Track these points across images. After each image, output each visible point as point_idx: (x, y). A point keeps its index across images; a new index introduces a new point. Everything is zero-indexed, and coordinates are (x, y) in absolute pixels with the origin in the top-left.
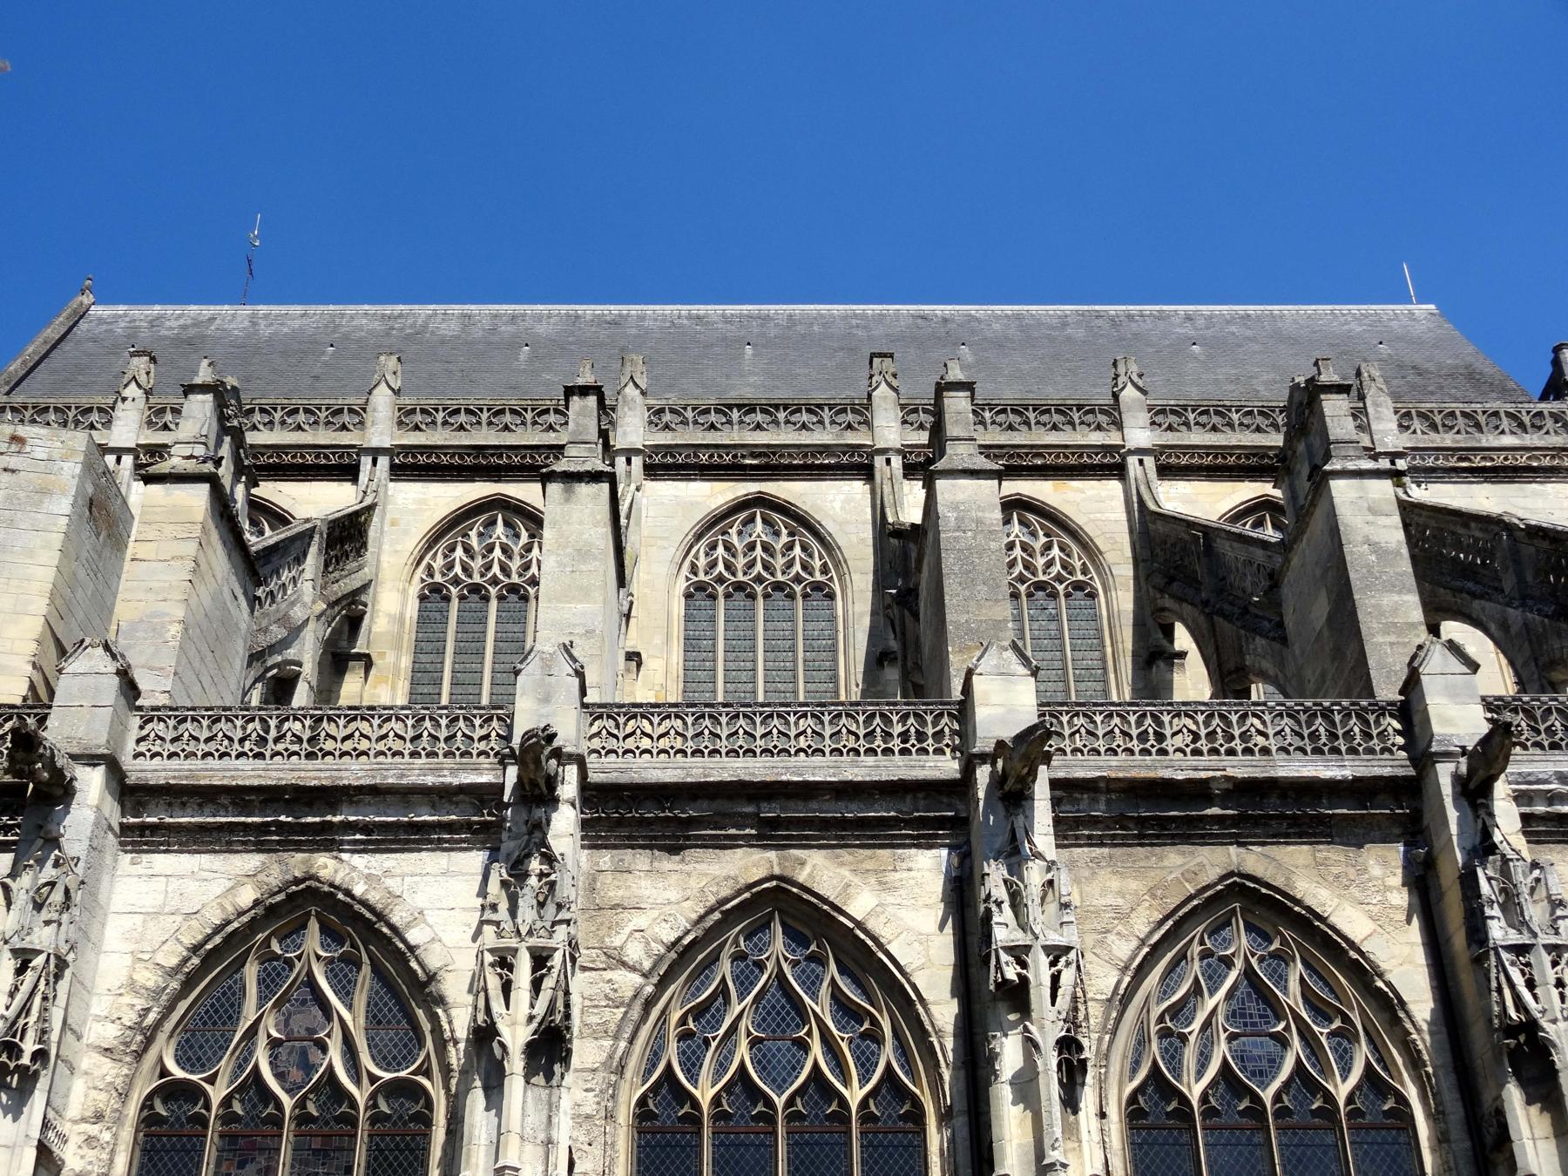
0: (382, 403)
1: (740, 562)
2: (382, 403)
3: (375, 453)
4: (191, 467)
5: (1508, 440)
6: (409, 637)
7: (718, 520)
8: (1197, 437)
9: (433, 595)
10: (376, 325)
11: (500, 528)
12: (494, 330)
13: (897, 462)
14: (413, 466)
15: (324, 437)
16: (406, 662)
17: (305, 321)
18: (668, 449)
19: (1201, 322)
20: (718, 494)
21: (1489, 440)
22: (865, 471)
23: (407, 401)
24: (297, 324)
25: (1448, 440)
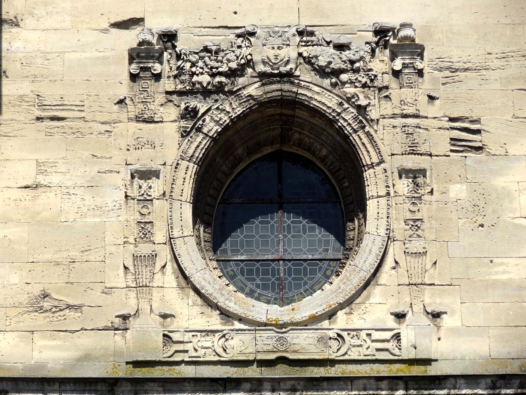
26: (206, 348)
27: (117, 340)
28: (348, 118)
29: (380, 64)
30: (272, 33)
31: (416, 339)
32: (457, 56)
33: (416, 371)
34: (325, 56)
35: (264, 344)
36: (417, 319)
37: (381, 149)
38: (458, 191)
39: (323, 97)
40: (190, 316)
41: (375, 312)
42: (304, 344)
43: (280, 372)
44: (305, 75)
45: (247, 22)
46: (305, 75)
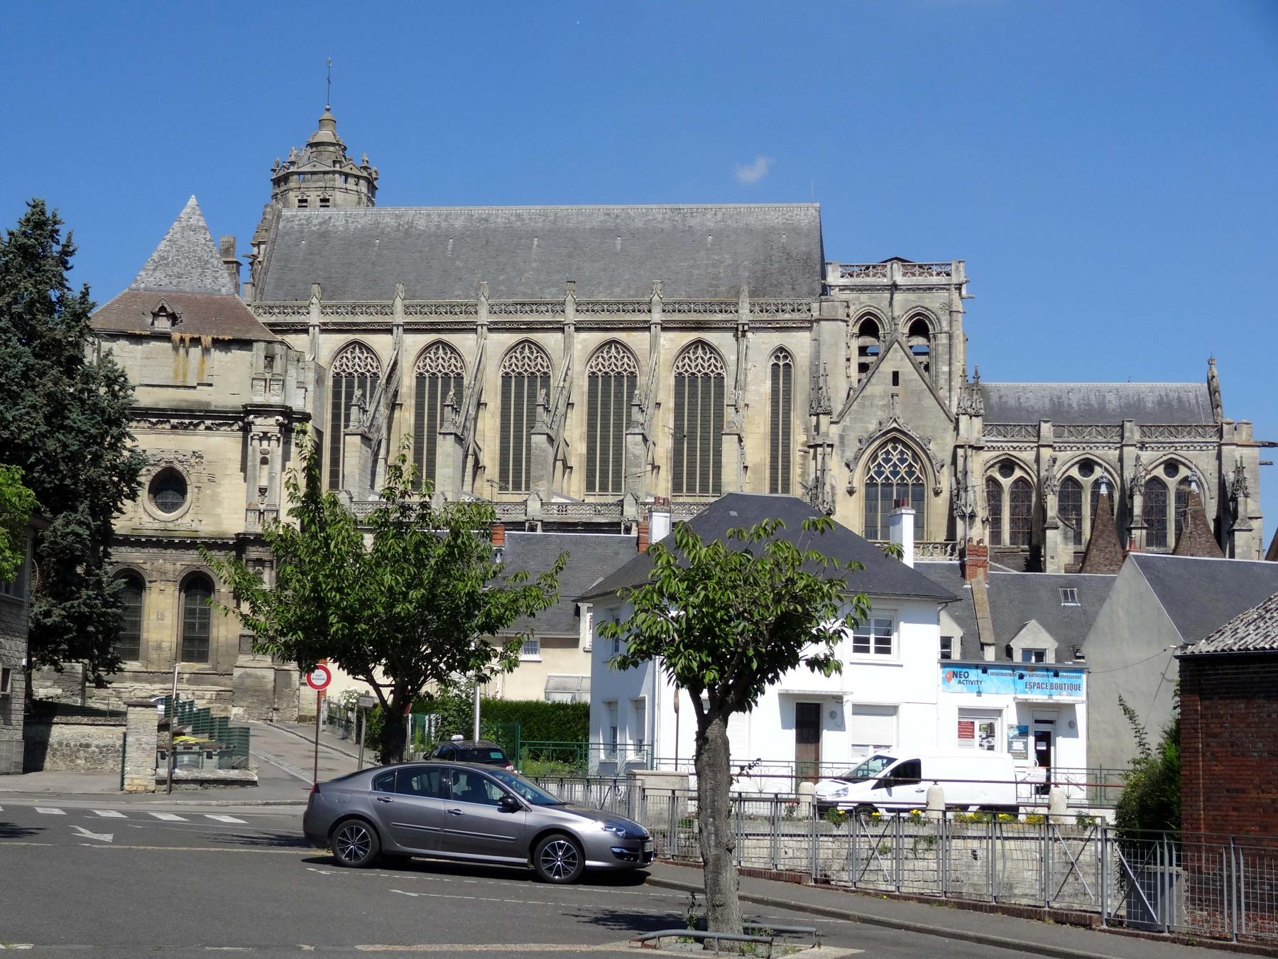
0: (399, 304)
1: (520, 364)
2: (399, 304)
3: (398, 326)
4: (355, 431)
5: (787, 316)
6: (414, 392)
7: (513, 348)
8: (677, 317)
9: (420, 378)
10: (393, 222)
11: (441, 351)
12: (438, 227)
13: (572, 328)
14: (411, 329)
15: (380, 319)
16: (413, 402)
17: (366, 219)
18: (496, 323)
19: (719, 216)
20: (513, 338)
21: (781, 316)
22: (562, 330)
23: (407, 302)
24: (362, 221)
25: (765, 316)
26: (149, 526)
27: (129, 523)
28: (184, 474)
29: (193, 460)
30: (169, 451)
31: (195, 526)
32: (211, 459)
33: (194, 535)
34: (181, 458)
35: (162, 526)
36: (196, 521)
37: (191, 481)
38: (208, 492)
39: (179, 467)
40: (146, 519)
41: (187, 519)
42: (171, 526)
43: (166, 534)
44: (176, 462)
45: (163, 447)
46: (176, 462)
